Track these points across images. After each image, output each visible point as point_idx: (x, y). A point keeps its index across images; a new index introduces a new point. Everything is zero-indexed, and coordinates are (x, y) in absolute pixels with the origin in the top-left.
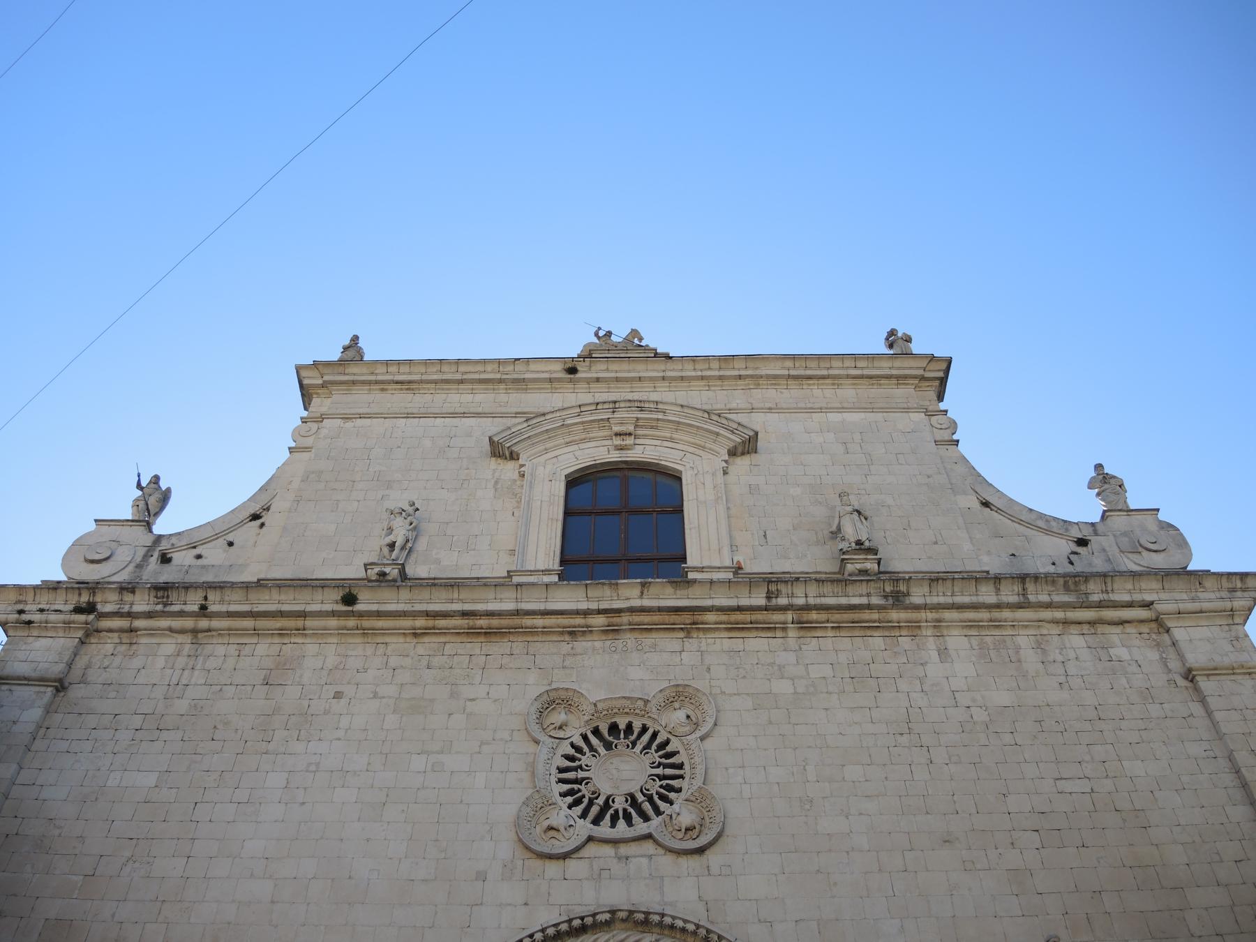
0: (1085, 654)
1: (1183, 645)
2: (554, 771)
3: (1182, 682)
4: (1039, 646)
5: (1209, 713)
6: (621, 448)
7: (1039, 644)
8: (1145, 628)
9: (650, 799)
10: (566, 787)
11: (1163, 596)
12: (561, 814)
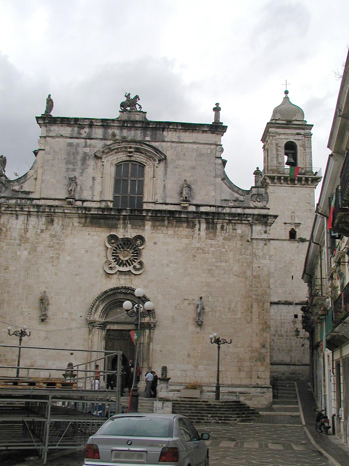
2: (111, 254)
6: (129, 156)
9: (131, 261)
10: (114, 257)
12: (114, 264)
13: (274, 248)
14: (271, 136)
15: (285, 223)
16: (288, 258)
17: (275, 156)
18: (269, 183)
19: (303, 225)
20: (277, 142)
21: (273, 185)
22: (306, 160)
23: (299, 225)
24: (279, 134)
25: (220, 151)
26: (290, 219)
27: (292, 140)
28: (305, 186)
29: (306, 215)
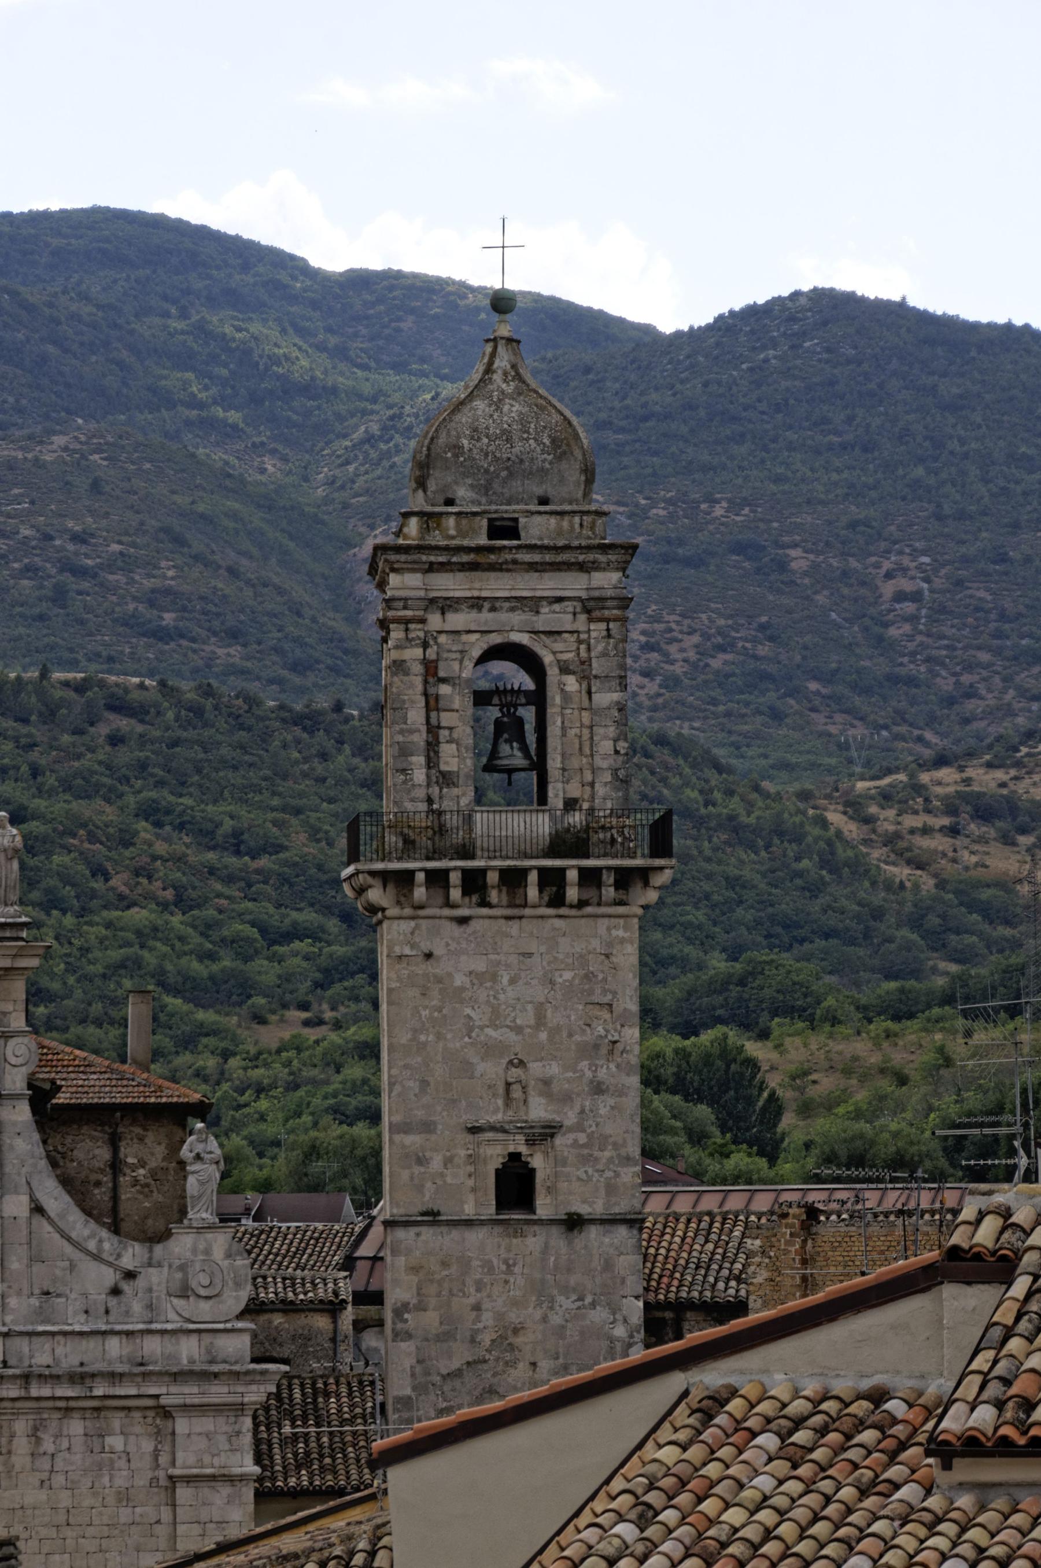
0: (78, 1443)
1: (179, 1440)
3: (163, 1482)
4: (35, 1435)
5: (175, 1523)
7: (36, 1429)
8: (151, 1414)
11: (173, 1389)
13: (415, 1269)
14: (398, 621)
15: (474, 1130)
16: (487, 1318)
17: (420, 739)
18: (384, 904)
19: (571, 1130)
20: (431, 653)
21: (408, 911)
22: (592, 755)
23: (552, 1135)
24: (446, 605)
25: (20, 1061)
26: (500, 1102)
27: (516, 637)
28: (589, 910)
29: (589, 1074)
